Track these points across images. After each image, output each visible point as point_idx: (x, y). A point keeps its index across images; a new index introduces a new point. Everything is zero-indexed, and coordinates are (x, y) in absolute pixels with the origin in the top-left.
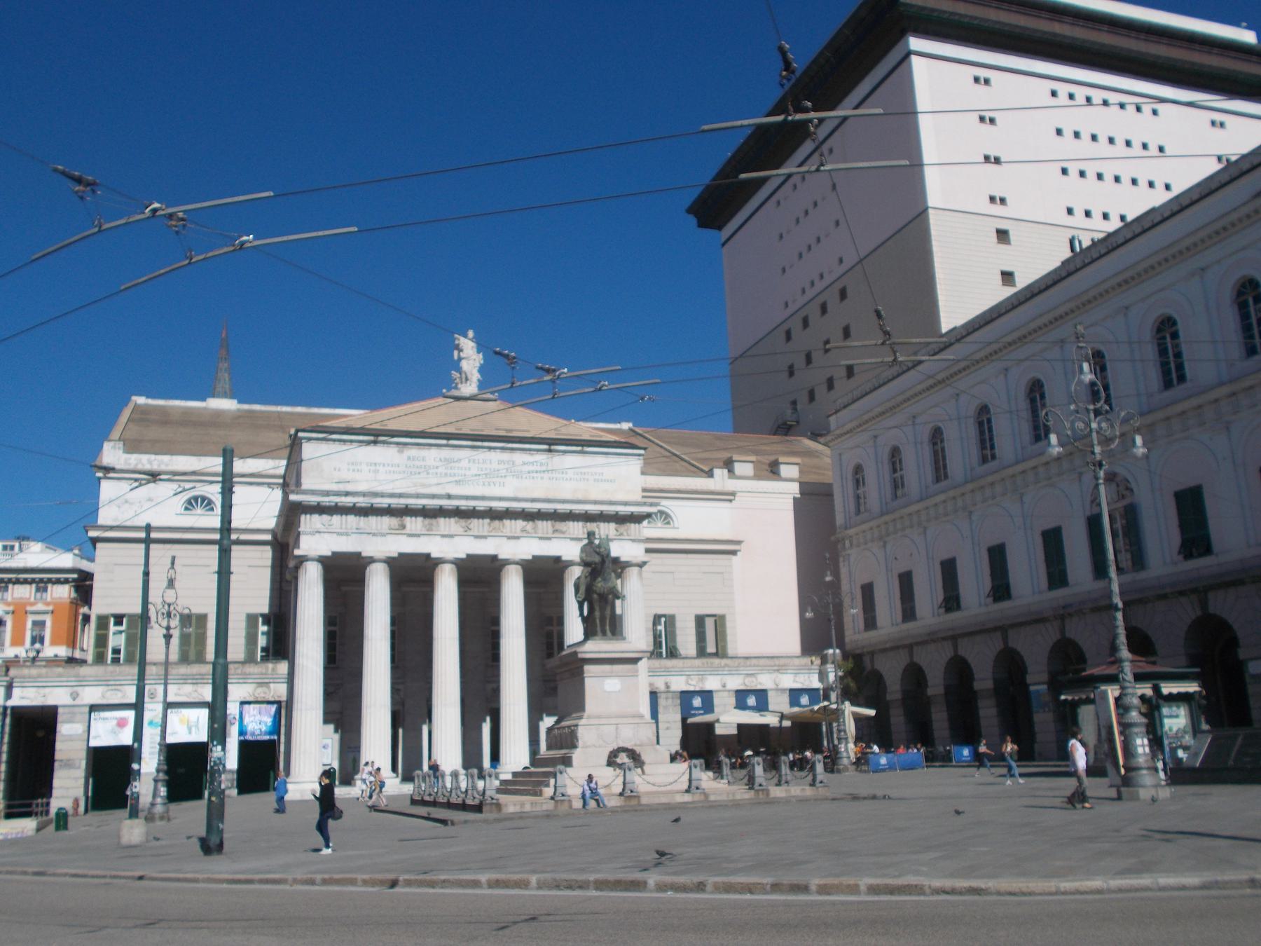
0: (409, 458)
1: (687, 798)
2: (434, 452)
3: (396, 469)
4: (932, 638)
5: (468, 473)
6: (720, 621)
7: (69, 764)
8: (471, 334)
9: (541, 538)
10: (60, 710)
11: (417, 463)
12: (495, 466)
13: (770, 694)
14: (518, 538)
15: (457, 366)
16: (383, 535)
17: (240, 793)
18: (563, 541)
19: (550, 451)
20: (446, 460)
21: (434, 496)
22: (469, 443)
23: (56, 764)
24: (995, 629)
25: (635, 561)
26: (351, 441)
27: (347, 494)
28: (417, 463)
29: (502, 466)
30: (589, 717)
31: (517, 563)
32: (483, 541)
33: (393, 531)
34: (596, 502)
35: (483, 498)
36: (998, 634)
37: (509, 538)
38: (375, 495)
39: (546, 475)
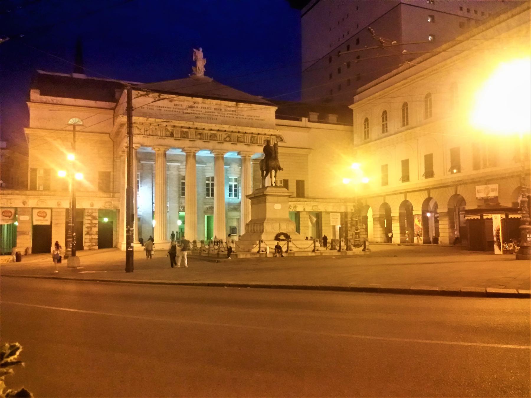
0: (175, 105)
1: (313, 254)
3: (169, 109)
4: (395, 193)
6: (303, 182)
7: (24, 233)
8: (201, 50)
10: (19, 210)
11: (180, 107)
12: (213, 110)
13: (323, 214)
15: (195, 64)
17: (99, 248)
19: (237, 105)
22: (201, 99)
23: (18, 233)
24: (425, 190)
28: (180, 107)
29: (216, 111)
30: (268, 220)
36: (426, 192)
37: (219, 143)
39: (235, 116)
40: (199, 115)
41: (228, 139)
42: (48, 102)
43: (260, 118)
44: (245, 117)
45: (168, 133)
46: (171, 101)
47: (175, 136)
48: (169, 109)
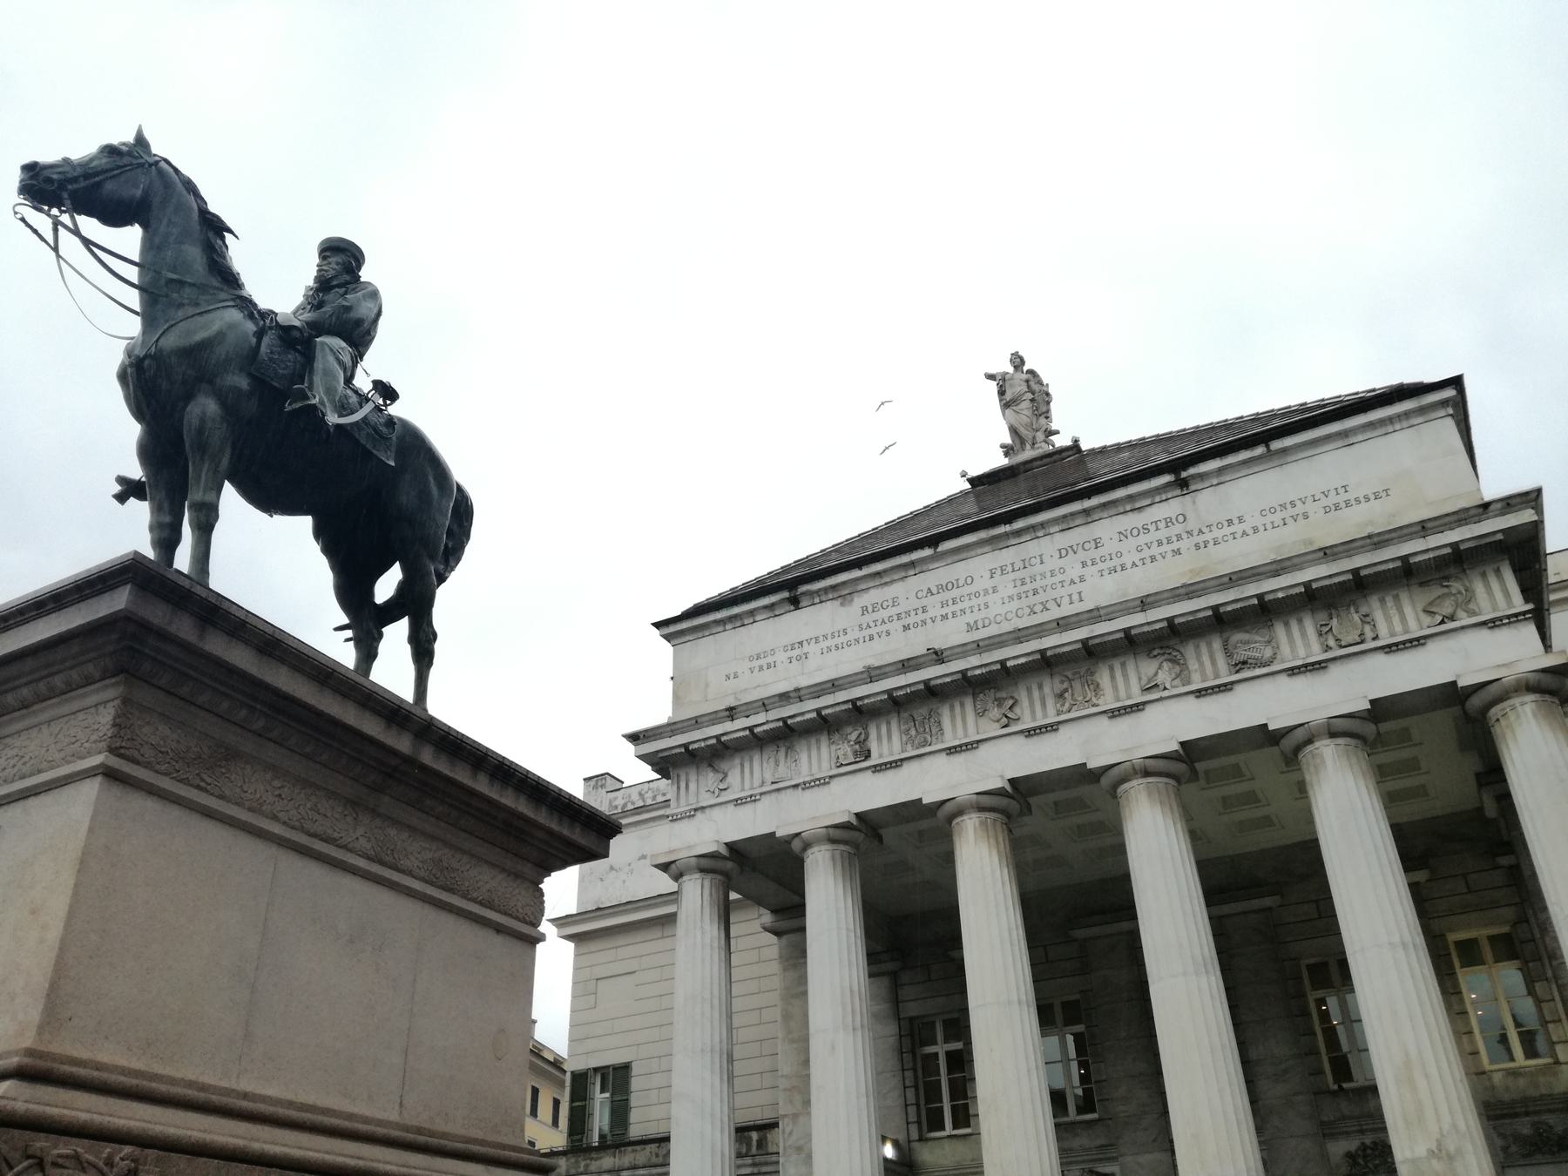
2: (916, 583)
3: (843, 639)
5: (991, 598)
9: (1200, 693)
11: (884, 614)
12: (1053, 563)
14: (1138, 708)
16: (822, 782)
18: (1267, 686)
19: (1183, 484)
20: (942, 588)
21: (906, 665)
25: (1509, 675)
26: (752, 613)
27: (732, 713)
28: (884, 614)
31: (1147, 773)
32: (1048, 740)
33: (843, 770)
34: (1327, 553)
35: (1019, 636)
37: (1114, 714)
38: (784, 697)
39: (1185, 544)
40: (978, 616)
41: (1164, 676)
42: (630, 807)
43: (1351, 496)
44: (1253, 520)
45: (845, 750)
46: (845, 599)
47: (874, 754)
48: (843, 639)
